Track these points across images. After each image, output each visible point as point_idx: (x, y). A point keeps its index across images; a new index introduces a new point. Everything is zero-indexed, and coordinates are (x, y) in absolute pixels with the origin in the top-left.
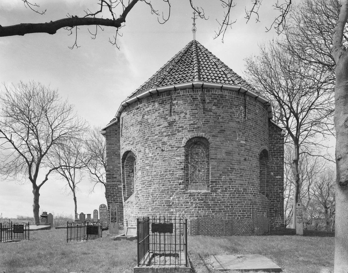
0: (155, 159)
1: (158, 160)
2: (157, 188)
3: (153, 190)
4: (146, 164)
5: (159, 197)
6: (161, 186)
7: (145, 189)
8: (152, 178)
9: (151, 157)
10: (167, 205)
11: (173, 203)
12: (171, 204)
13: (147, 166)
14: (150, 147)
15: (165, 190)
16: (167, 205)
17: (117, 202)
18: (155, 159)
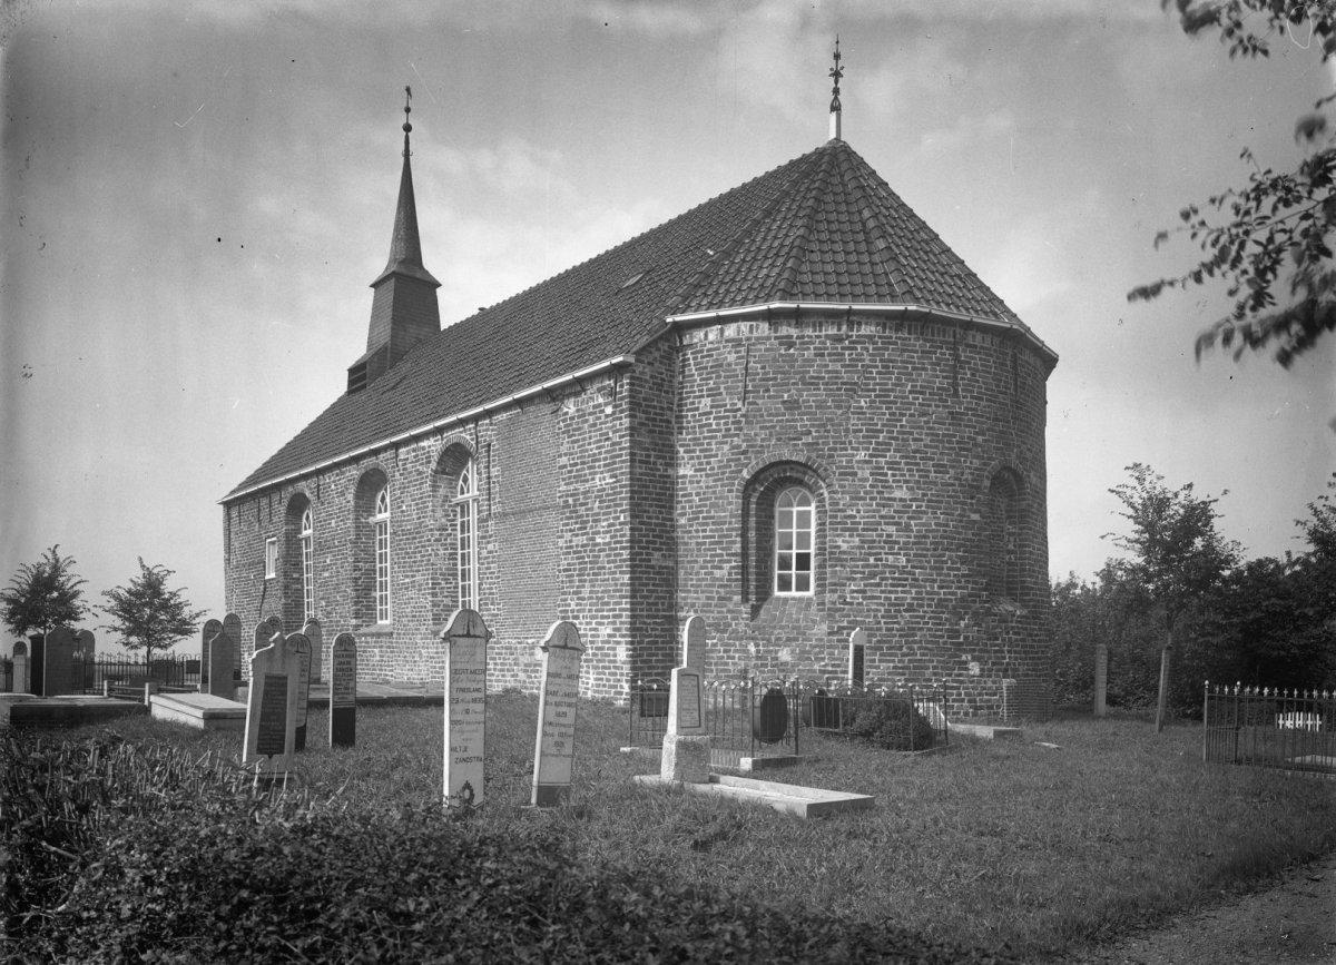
0: (914, 508)
1: (925, 513)
2: (927, 593)
3: (913, 598)
4: (882, 517)
5: (930, 618)
6: (936, 589)
7: (882, 592)
8: (908, 561)
9: (901, 500)
10: (952, 643)
11: (966, 638)
12: (961, 640)
13: (886, 524)
14: (899, 469)
15: (946, 600)
16: (952, 643)
17: (656, 617)
18: (914, 508)
